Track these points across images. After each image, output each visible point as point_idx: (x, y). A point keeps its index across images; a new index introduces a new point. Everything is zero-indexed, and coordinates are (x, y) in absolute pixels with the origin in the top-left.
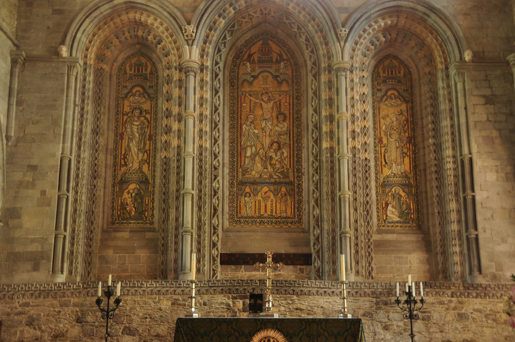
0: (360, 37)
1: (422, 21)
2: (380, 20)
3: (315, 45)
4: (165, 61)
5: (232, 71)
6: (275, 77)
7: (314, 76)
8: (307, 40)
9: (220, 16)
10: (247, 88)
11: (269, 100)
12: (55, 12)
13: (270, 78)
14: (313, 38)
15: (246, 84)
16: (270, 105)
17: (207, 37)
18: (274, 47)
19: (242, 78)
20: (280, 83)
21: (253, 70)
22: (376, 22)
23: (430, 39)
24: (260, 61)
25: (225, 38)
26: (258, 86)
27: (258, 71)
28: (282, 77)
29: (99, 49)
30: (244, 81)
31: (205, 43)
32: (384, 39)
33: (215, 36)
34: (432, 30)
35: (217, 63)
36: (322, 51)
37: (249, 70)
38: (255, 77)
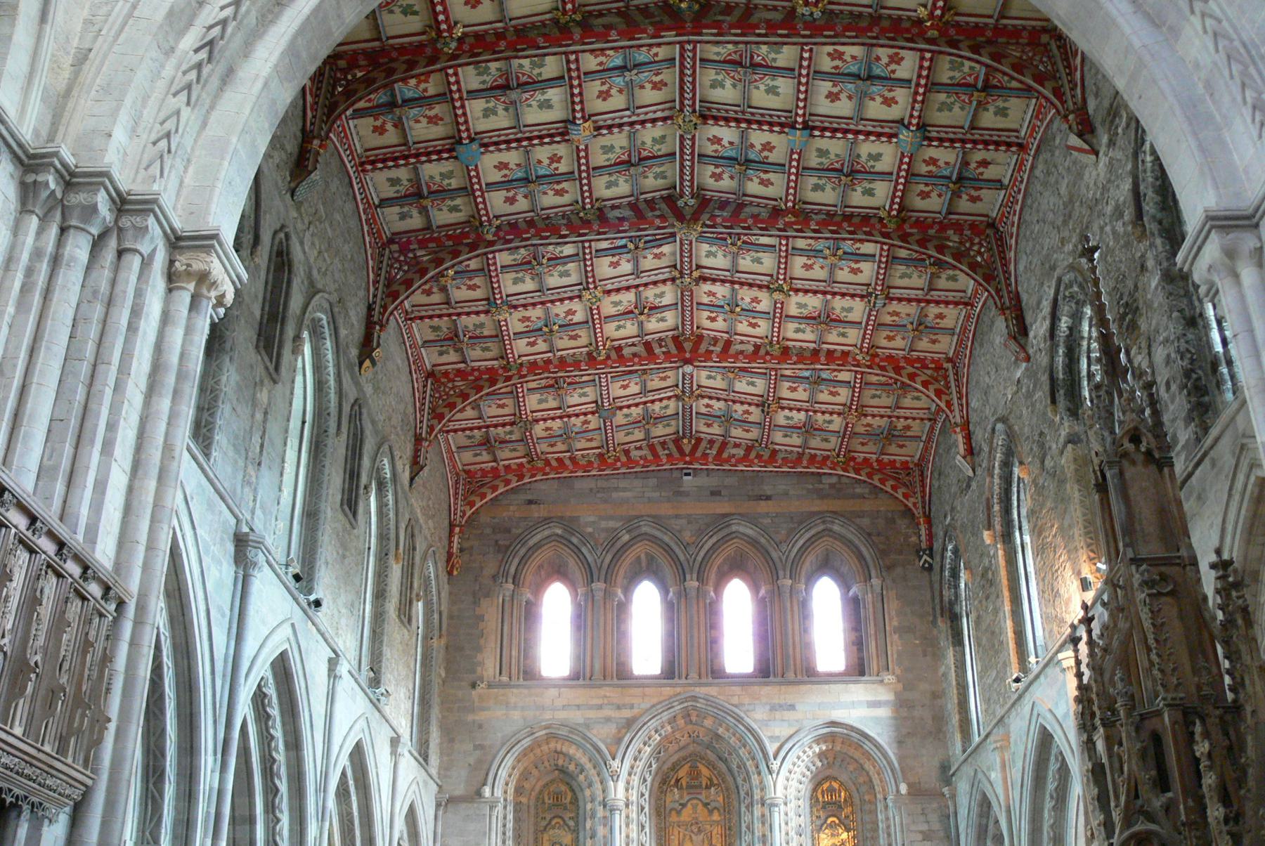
0: (794, 764)
1: (859, 747)
2: (814, 746)
3: (748, 773)
4: (587, 793)
5: (658, 799)
6: (706, 805)
7: (747, 807)
8: (739, 767)
9: (645, 744)
10: (674, 818)
11: (700, 831)
12: (476, 747)
13: (700, 806)
14: (745, 764)
15: (673, 813)
16: (701, 837)
17: (632, 767)
18: (705, 771)
19: (669, 805)
20: (711, 812)
21: (681, 797)
22: (810, 747)
23: (868, 766)
24: (689, 787)
25: (650, 766)
26: (686, 815)
27: (686, 798)
28: (713, 804)
29: (519, 781)
30: (671, 810)
31: (630, 774)
32: (819, 764)
33: (640, 764)
34: (868, 756)
35: (643, 795)
36: (755, 779)
37: (677, 797)
38: (684, 805)
